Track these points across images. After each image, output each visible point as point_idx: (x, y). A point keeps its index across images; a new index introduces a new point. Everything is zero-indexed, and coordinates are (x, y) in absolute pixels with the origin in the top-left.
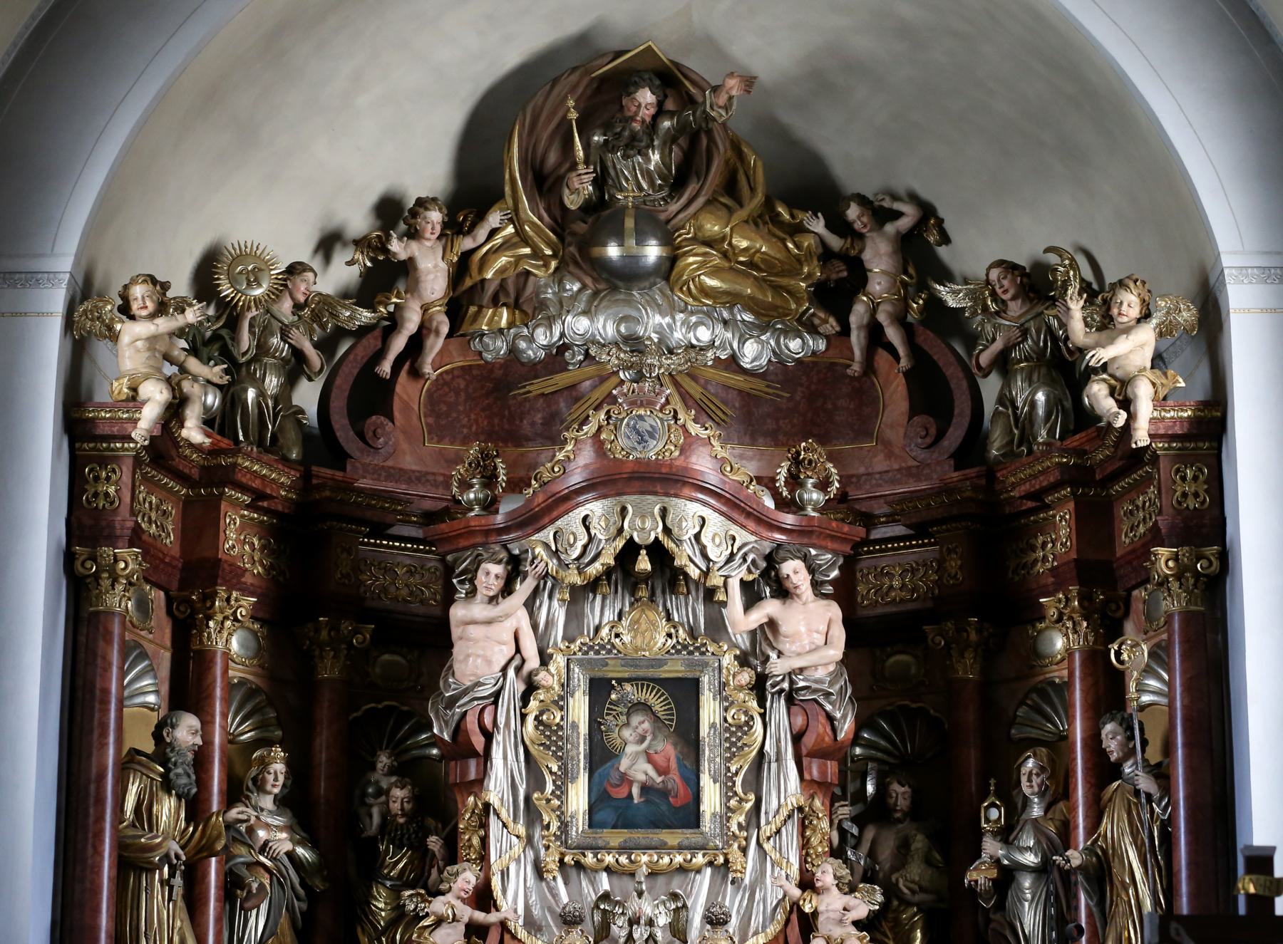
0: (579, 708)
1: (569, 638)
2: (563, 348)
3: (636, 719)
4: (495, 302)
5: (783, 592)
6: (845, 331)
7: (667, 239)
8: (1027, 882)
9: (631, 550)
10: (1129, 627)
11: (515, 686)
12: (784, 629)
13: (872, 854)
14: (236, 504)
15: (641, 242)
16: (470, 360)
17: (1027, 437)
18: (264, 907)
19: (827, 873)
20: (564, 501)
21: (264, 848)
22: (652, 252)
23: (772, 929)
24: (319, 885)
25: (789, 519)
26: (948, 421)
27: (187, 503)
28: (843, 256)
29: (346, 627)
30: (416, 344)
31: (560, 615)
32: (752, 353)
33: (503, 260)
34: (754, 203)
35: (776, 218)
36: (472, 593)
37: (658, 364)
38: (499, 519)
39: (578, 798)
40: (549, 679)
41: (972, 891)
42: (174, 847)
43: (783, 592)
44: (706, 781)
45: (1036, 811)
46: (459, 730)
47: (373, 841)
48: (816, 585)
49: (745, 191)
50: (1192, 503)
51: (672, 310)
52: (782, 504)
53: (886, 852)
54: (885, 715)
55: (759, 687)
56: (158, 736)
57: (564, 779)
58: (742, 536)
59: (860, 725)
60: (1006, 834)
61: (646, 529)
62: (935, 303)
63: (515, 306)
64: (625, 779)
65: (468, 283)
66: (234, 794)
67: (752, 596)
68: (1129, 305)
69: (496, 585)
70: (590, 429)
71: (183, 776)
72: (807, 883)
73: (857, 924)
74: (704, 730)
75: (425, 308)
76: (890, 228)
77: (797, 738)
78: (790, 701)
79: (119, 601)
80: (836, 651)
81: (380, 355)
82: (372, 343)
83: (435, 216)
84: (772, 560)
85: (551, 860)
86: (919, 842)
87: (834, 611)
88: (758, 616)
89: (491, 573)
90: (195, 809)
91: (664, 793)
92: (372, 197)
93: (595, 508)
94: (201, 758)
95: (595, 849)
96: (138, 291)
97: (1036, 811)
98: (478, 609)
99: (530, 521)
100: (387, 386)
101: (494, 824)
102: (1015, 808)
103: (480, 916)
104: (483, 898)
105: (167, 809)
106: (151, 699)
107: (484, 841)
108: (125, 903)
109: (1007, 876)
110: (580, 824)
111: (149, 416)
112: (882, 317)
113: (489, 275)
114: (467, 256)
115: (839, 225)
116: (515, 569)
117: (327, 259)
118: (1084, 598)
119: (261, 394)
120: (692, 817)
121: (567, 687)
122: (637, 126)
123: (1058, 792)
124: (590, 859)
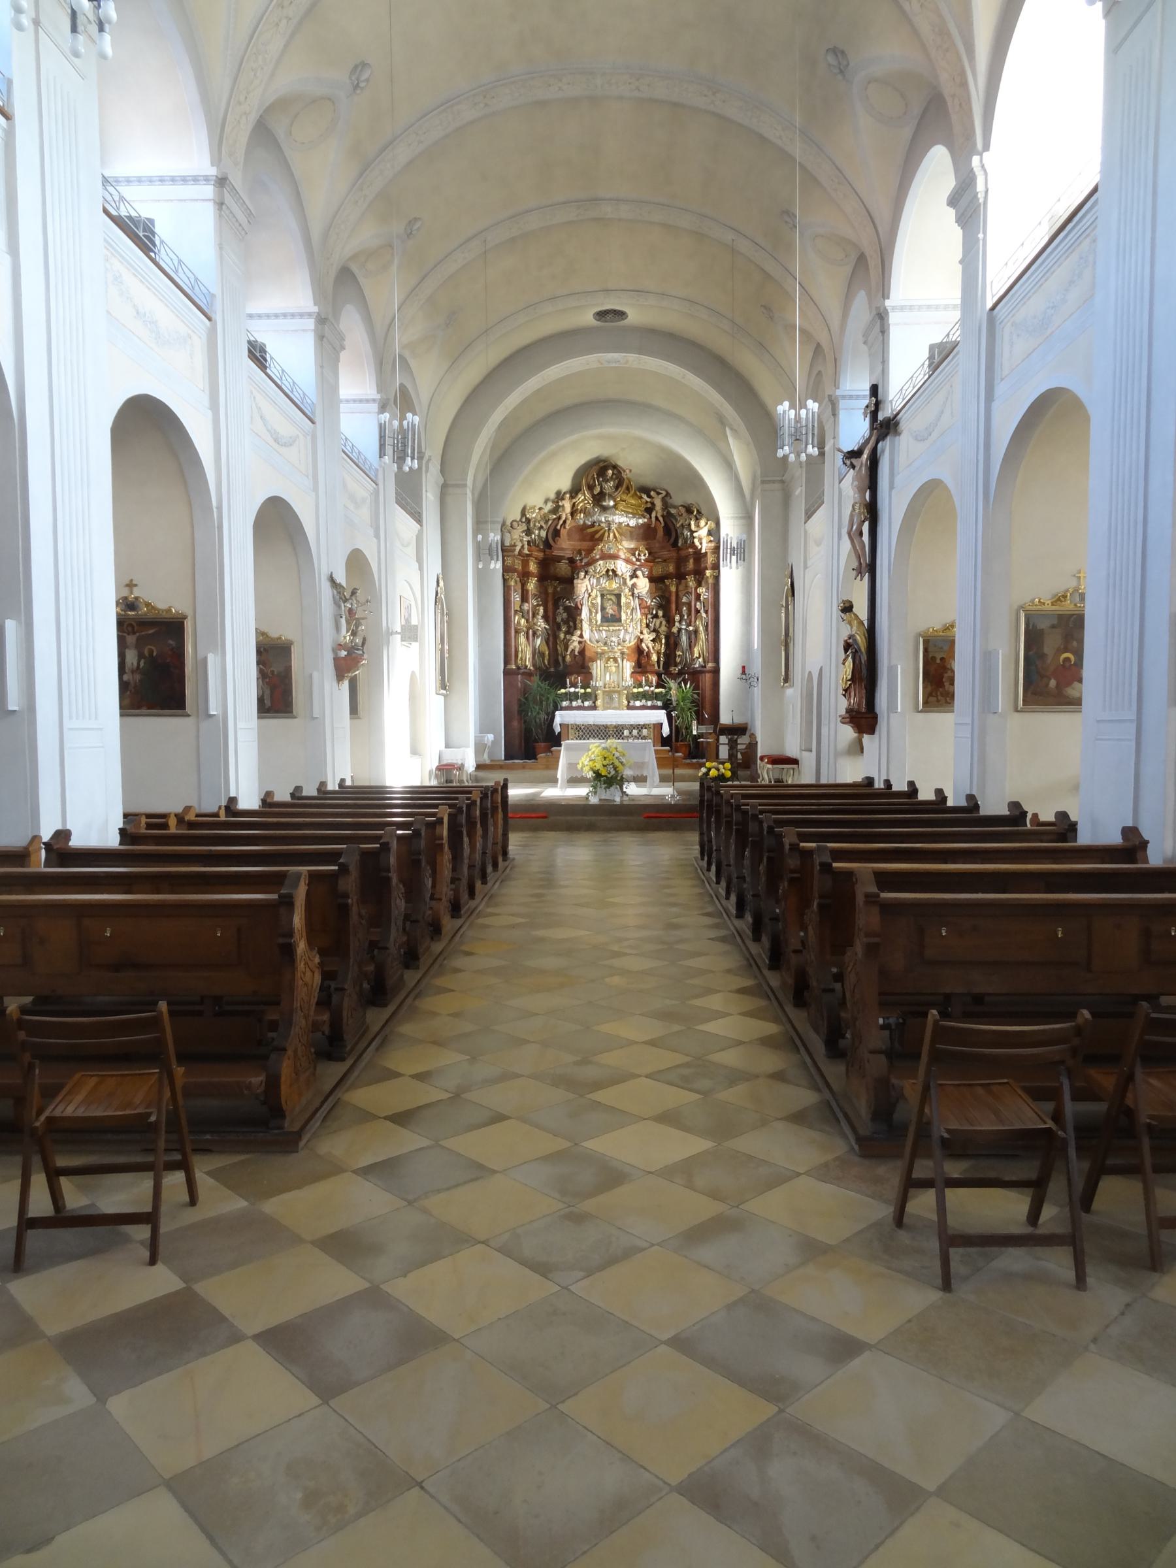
0: (599, 600)
1: (596, 586)
2: (594, 522)
3: (610, 601)
4: (580, 513)
5: (637, 577)
6: (651, 518)
7: (615, 501)
8: (683, 631)
9: (608, 571)
10: (703, 583)
11: (586, 595)
12: (638, 584)
13: (655, 625)
14: (532, 560)
15: (609, 502)
16: (576, 524)
17: (686, 542)
18: (540, 639)
19: (645, 631)
20: (597, 560)
21: (540, 626)
22: (612, 503)
23: (635, 641)
24: (550, 632)
25: (638, 563)
26: (671, 538)
27: (523, 561)
28: (651, 502)
29: (553, 582)
30: (565, 522)
31: (595, 581)
32: (633, 523)
33: (581, 504)
34: (632, 492)
35: (636, 494)
36: (578, 578)
37: (614, 527)
38: (583, 564)
39: (599, 616)
40: (593, 594)
41: (673, 633)
42: (525, 629)
43: (637, 577)
44: (622, 613)
45: (686, 617)
46: (576, 605)
47: (560, 623)
48: (643, 575)
49: (631, 489)
50: (713, 562)
51: (615, 514)
52: (638, 560)
53: (658, 625)
54: (658, 597)
55: (633, 595)
56: (520, 607)
57: (597, 613)
58: (629, 566)
59: (652, 601)
60: (680, 622)
61: (612, 567)
62: (669, 513)
63: (584, 513)
64: (608, 613)
65: (574, 509)
66: (534, 616)
67: (632, 577)
68: (702, 523)
69: (582, 577)
70: (600, 547)
71: (525, 615)
72: (641, 633)
73: (651, 641)
74: (622, 604)
75: (566, 514)
76: (660, 496)
77: (640, 605)
78: (638, 598)
79: (512, 583)
80: (647, 588)
81: (557, 525)
82: (556, 522)
83: (568, 496)
84: (635, 571)
85: (594, 629)
86: (664, 623)
87: (647, 580)
88: (632, 582)
89: (582, 574)
90: (527, 621)
91: (615, 616)
92: (555, 491)
93: (601, 562)
94: (528, 611)
95: (602, 626)
96: (514, 523)
97: (686, 617)
98: (579, 581)
99: (589, 564)
100: (559, 531)
101: (583, 622)
102: (682, 617)
103: (581, 640)
104: (581, 636)
105: (523, 621)
106: (518, 599)
107: (581, 625)
108: (516, 639)
109: (680, 630)
110: (599, 622)
111: (518, 548)
112: (659, 516)
113: (579, 507)
114: (574, 503)
115: (649, 496)
116: (586, 573)
117: (546, 505)
118: (695, 578)
119: (535, 536)
120: (619, 620)
121: (597, 596)
122: (608, 478)
123: (689, 614)
124: (601, 628)
